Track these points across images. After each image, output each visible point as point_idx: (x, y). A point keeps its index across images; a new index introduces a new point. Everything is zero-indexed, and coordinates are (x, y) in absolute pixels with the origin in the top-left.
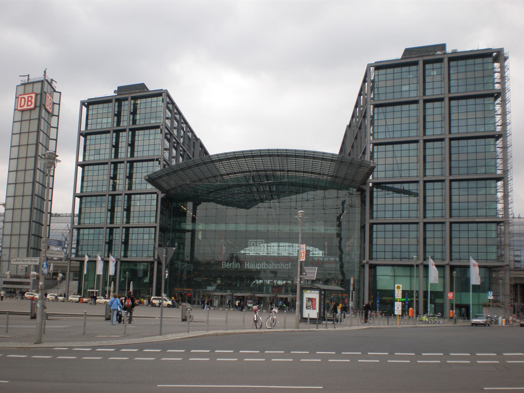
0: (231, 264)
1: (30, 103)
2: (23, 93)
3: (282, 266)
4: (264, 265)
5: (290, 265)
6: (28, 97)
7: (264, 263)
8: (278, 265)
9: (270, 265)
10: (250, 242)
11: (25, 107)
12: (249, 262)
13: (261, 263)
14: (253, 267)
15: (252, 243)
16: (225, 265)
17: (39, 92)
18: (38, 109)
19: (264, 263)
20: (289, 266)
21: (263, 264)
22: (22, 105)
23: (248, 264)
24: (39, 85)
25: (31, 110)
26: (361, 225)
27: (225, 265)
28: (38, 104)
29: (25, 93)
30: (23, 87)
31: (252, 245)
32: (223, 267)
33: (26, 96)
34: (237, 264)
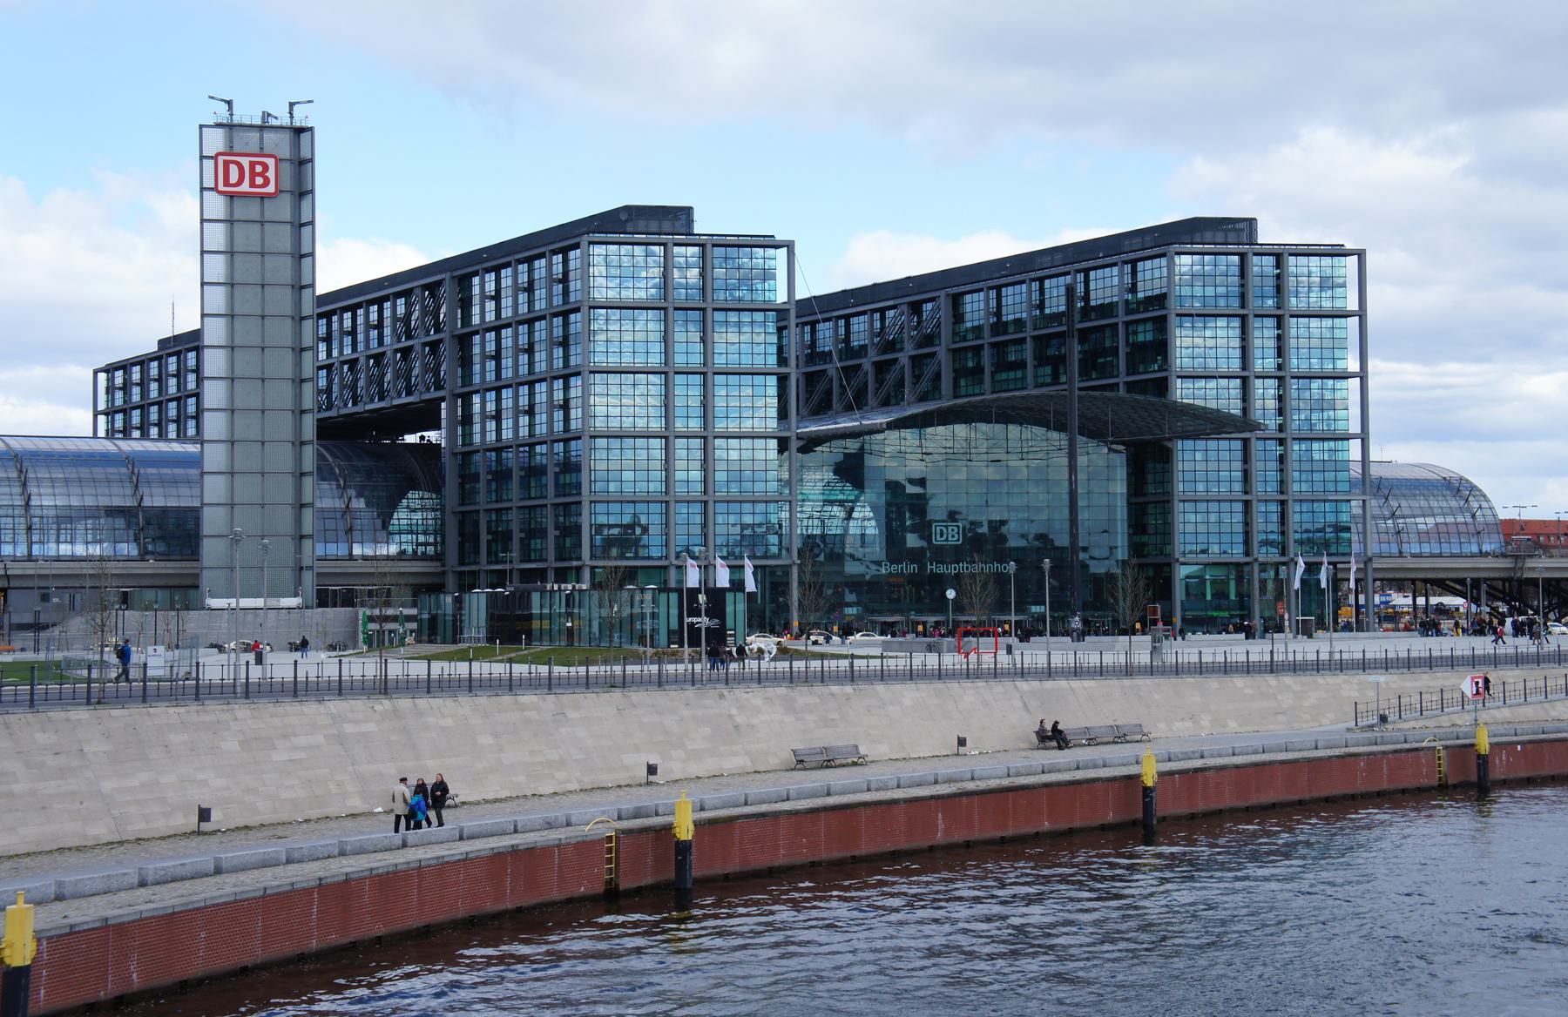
1: (259, 180)
2: (221, 149)
6: (253, 165)
11: (245, 187)
15: (938, 528)
17: (285, 152)
18: (286, 202)
21: (961, 565)
22: (234, 178)
24: (286, 138)
25: (262, 197)
26: (1128, 499)
28: (287, 183)
29: (236, 150)
30: (220, 132)
31: (938, 532)
33: (245, 161)
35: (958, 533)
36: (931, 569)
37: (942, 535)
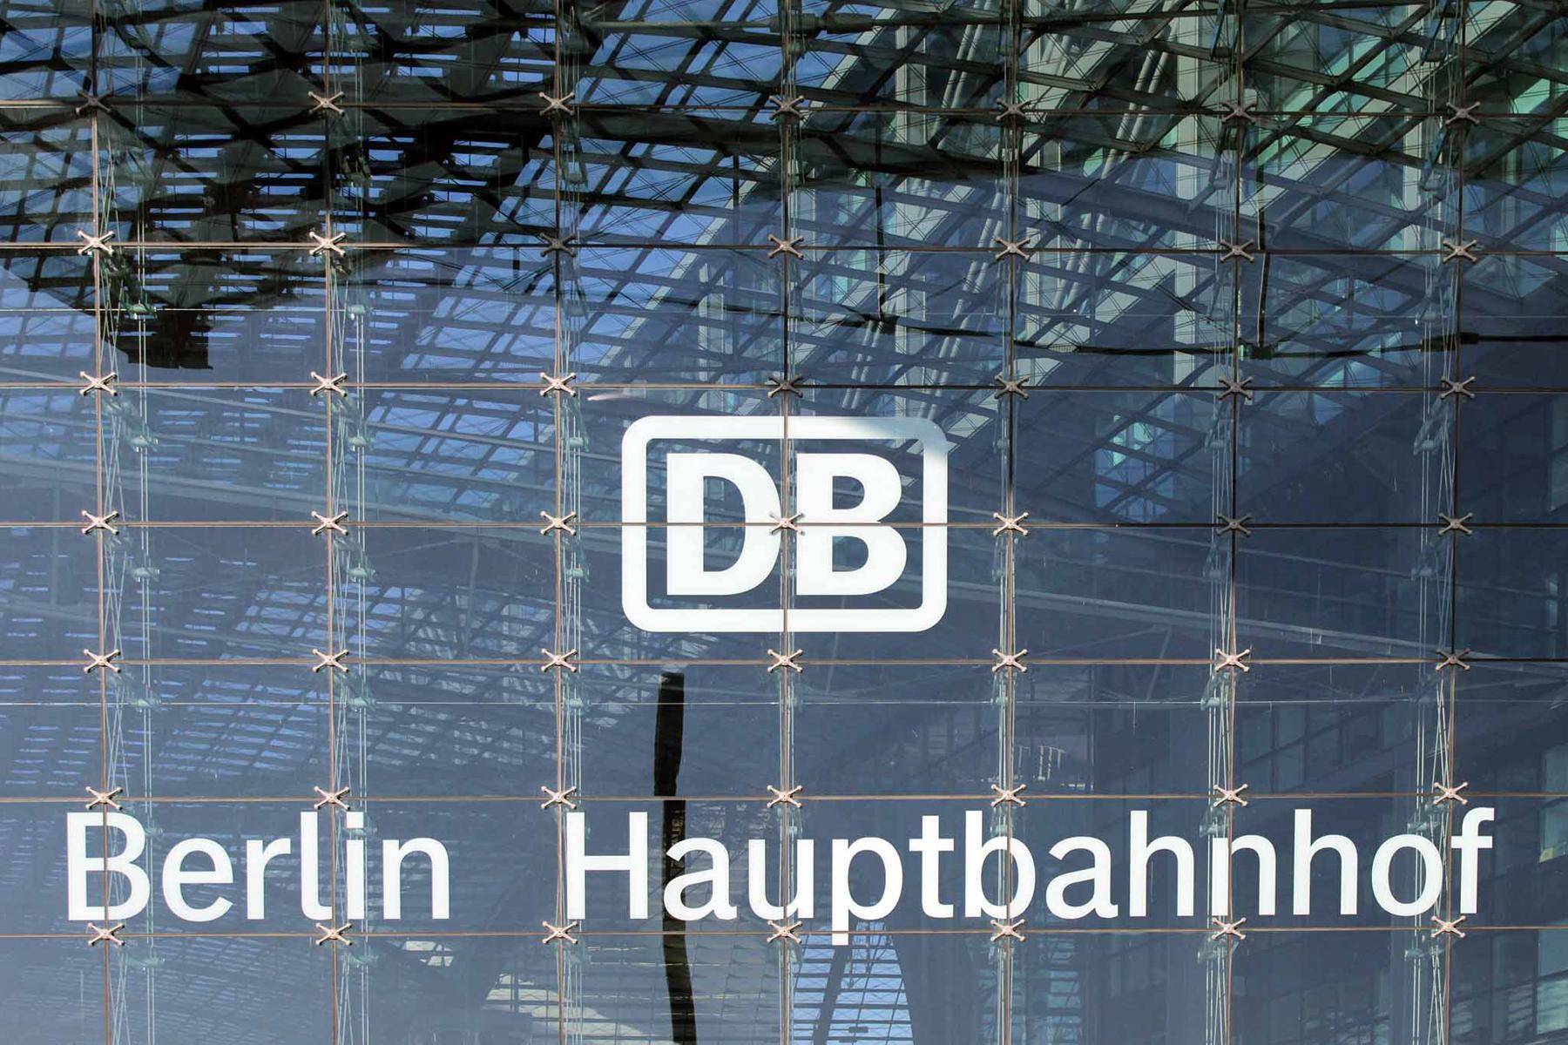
0: (258, 855)
3: (1326, 865)
4: (952, 866)
5: (1471, 842)
7: (953, 828)
8: (1245, 865)
9: (1083, 859)
10: (657, 450)
13: (902, 832)
14: (739, 896)
16: (121, 863)
19: (953, 828)
20: (1453, 862)
21: (930, 843)
23: (622, 848)
27: (121, 863)
32: (79, 909)
34: (393, 853)
35: (906, 518)
36: (608, 889)
37: (719, 555)
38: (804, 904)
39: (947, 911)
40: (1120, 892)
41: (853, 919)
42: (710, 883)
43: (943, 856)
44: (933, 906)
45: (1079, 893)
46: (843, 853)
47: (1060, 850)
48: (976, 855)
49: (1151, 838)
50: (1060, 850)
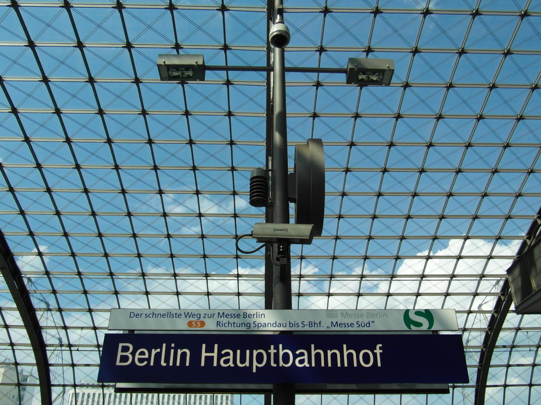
3: (350, 356)
7: (277, 348)
8: (334, 356)
12: (216, 346)
13: (267, 349)
19: (277, 348)
21: (272, 351)
36: (209, 360)
38: (247, 364)
39: (275, 365)
40: (310, 362)
41: (256, 366)
42: (230, 359)
43: (274, 353)
44: (273, 365)
45: (302, 362)
46: (255, 353)
47: (298, 352)
48: (281, 353)
49: (315, 350)
50: (298, 352)
